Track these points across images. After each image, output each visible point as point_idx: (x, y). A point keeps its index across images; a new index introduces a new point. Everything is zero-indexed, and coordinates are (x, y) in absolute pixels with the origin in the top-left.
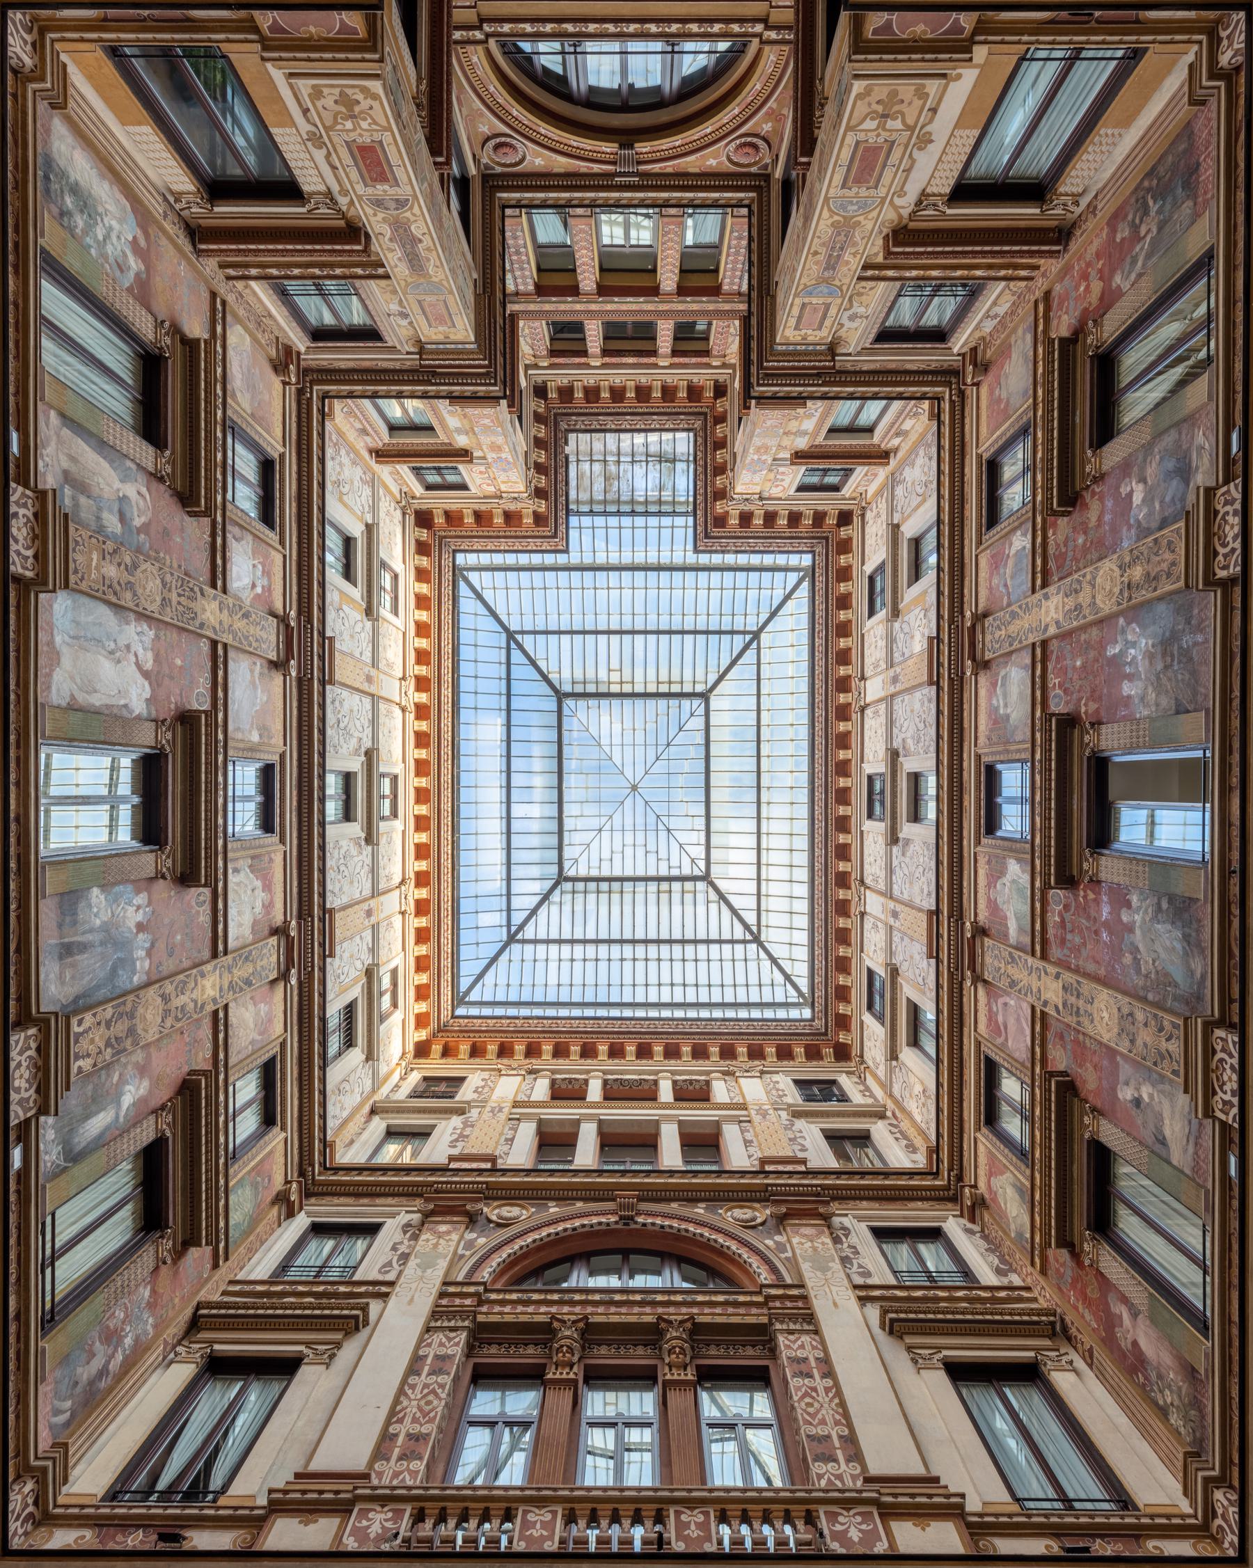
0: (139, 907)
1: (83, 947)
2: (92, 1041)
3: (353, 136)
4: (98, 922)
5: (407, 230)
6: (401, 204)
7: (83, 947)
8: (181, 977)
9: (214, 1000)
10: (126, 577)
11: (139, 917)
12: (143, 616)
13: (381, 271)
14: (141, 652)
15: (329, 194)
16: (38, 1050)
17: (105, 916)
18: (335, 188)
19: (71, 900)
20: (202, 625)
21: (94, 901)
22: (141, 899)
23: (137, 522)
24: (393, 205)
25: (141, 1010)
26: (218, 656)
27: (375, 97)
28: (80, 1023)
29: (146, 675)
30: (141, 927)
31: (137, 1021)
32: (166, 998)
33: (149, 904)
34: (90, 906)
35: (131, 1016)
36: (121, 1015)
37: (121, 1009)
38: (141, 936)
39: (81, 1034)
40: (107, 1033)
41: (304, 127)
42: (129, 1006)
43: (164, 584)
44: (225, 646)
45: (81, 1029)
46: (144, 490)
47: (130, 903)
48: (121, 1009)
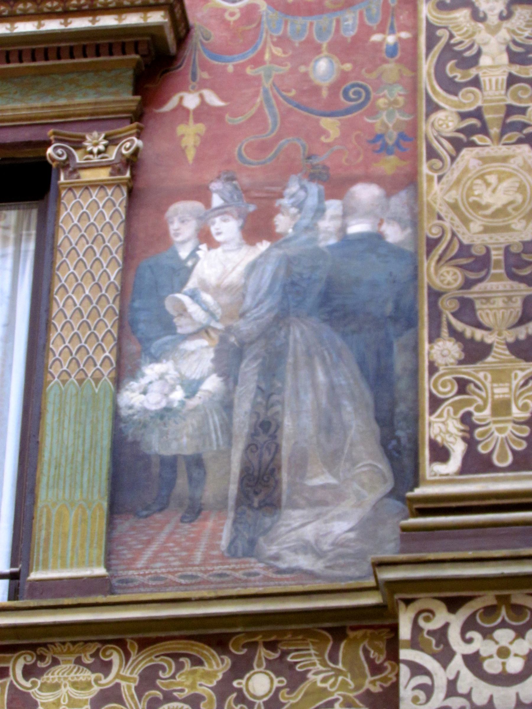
0: (205, 237)
1: (266, 428)
2: (501, 408)
4: (213, 384)
7: (266, 428)
8: (426, 66)
11: (227, 228)
16: (453, 605)
17: (198, 359)
19: (136, 480)
21: (153, 401)
22: (181, 222)
25: (473, 234)
28: (441, 454)
30: (257, 228)
31: (497, 243)
32: (473, 128)
33: (202, 194)
34: (166, 413)
35: (476, 264)
36: (466, 310)
37: (448, 306)
38: (283, 223)
39: (471, 443)
40: (500, 353)
42: (449, 278)
45: (458, 450)
47: (181, 273)
48: (448, 306)
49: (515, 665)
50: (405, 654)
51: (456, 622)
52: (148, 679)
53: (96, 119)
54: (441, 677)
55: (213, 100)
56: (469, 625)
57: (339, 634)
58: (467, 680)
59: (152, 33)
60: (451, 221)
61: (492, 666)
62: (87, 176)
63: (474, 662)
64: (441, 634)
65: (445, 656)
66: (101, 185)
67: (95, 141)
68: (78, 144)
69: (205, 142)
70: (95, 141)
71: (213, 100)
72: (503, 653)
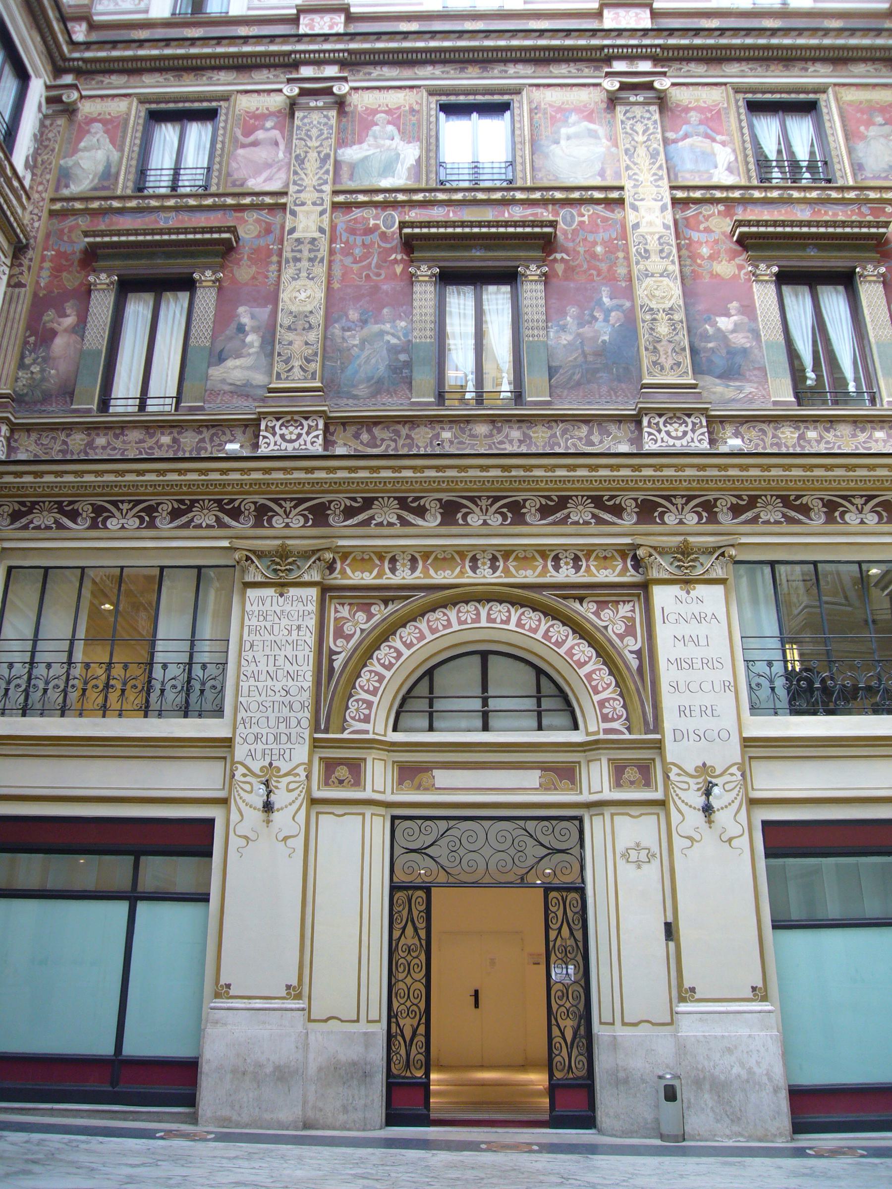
9: (663, 208)
20: (321, 230)
44: (336, 193)
49: (680, 434)
50: (646, 429)
51: (662, 420)
52: (564, 432)
53: (533, 260)
54: (659, 437)
55: (565, 257)
56: (665, 422)
57: (620, 422)
58: (666, 438)
59: (551, 233)
60: (646, 301)
61: (673, 434)
62: (530, 278)
63: (668, 433)
64: (657, 424)
65: (659, 431)
66: (536, 281)
67: (533, 267)
68: (528, 267)
69: (565, 271)
70: (533, 267)
71: (565, 257)
72: (676, 430)
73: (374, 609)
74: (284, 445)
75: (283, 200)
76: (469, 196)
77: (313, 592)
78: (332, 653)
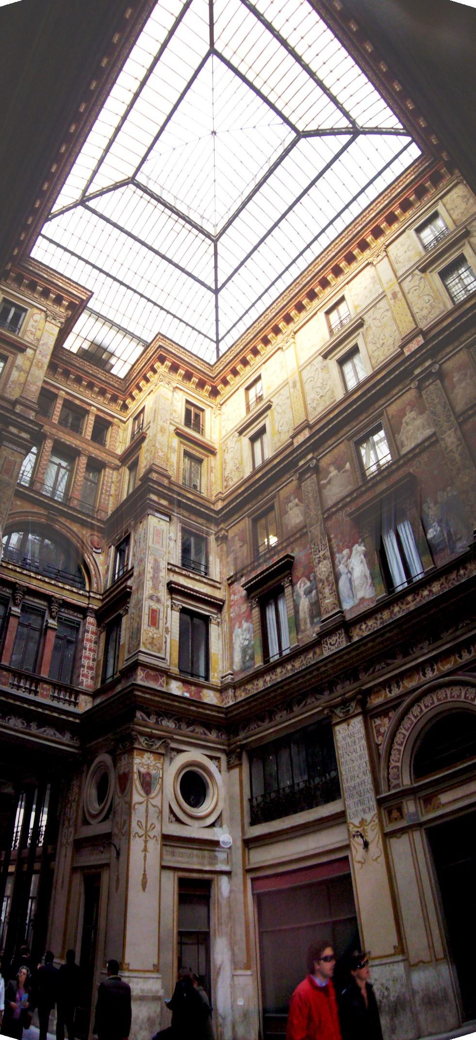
3: (156, 631)
5: (154, 585)
6: (151, 597)
10: (326, 583)
12: (334, 566)
13: (170, 567)
14: (345, 559)
15: (172, 609)
18: (169, 609)
23: (308, 584)
24: (154, 598)
26: (328, 514)
27: (144, 644)
29: (351, 551)
41: (168, 637)
43: (319, 562)
46: (298, 585)
73: (390, 715)
74: (332, 647)
75: (305, 530)
76: (358, 492)
77: (360, 719)
78: (378, 745)
